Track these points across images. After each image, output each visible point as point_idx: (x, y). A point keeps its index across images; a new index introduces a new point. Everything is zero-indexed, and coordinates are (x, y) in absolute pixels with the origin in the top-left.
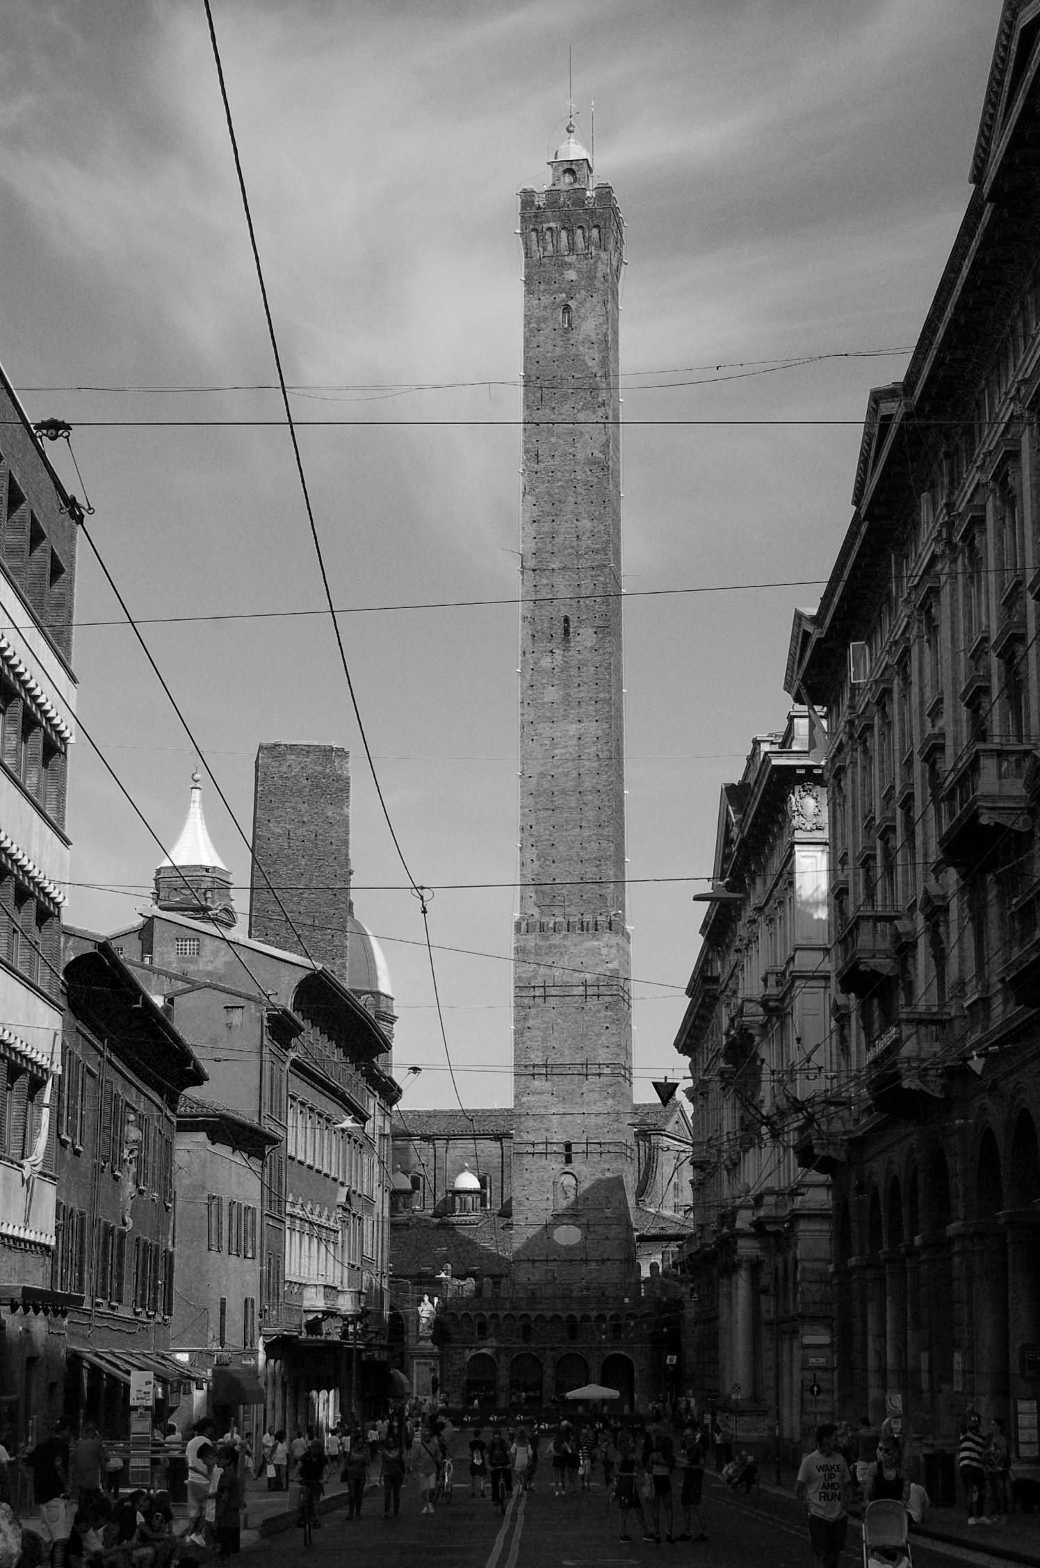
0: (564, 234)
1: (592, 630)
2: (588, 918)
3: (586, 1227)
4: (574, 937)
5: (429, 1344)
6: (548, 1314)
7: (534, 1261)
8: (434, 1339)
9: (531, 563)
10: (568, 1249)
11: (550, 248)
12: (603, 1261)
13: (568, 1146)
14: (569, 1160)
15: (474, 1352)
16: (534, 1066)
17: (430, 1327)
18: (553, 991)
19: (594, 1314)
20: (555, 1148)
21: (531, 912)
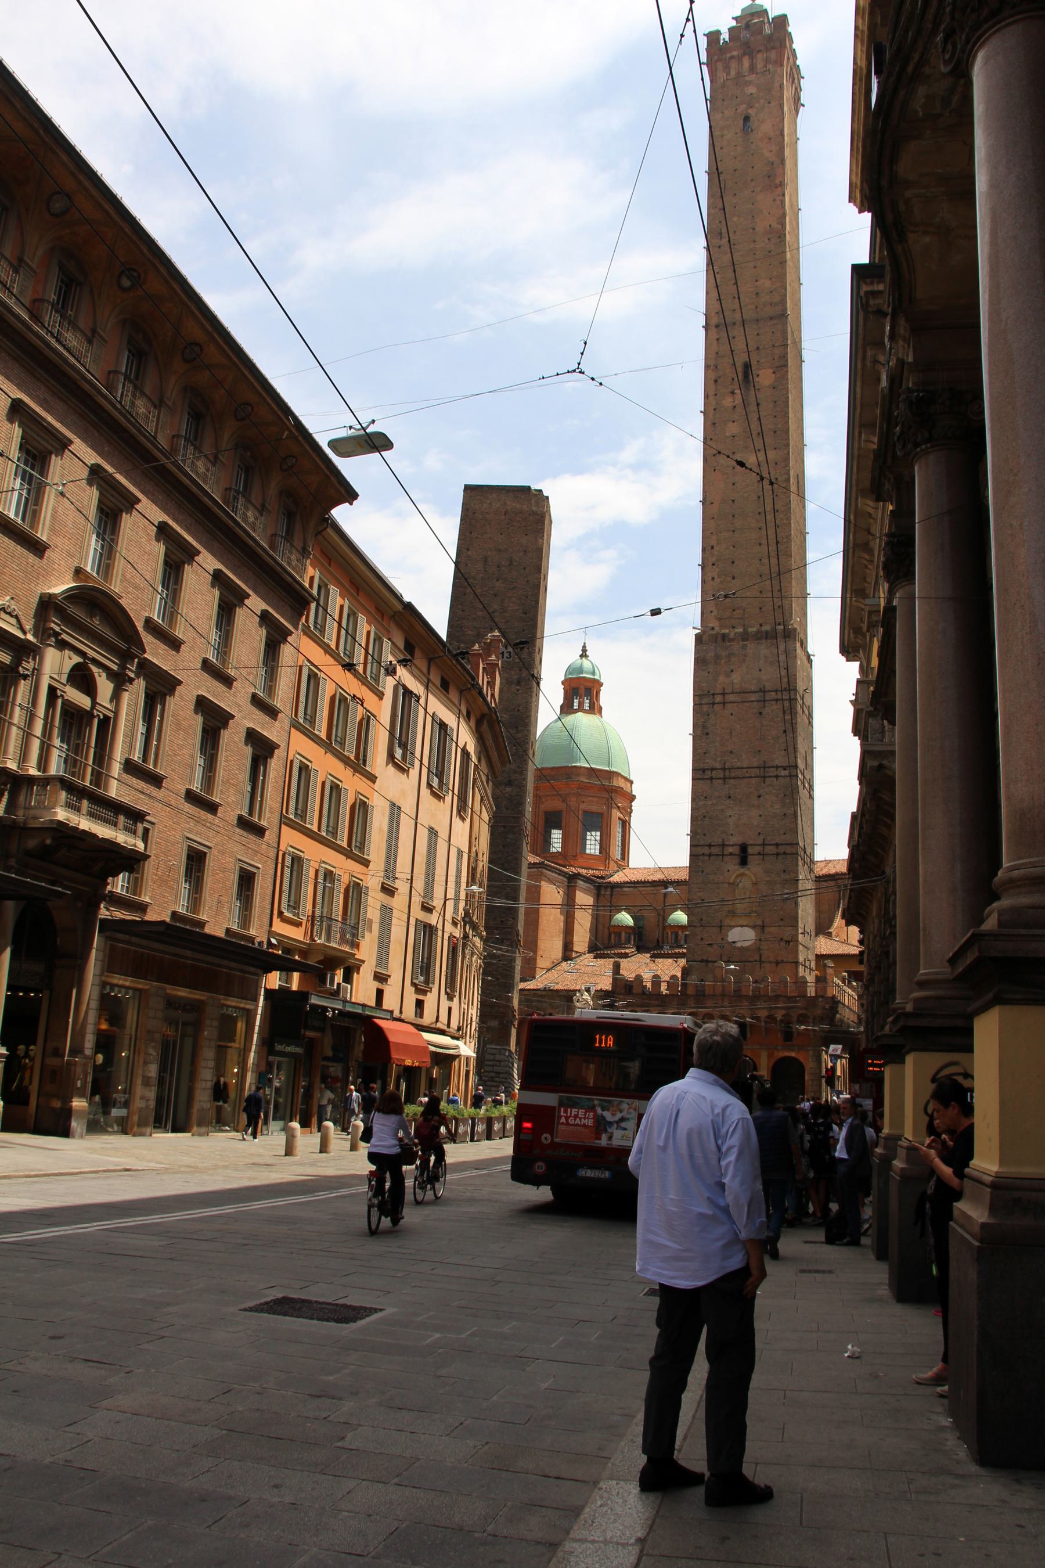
0: (746, 63)
1: (771, 371)
2: (767, 628)
4: (751, 646)
7: (707, 961)
9: (714, 321)
11: (733, 73)
13: (744, 848)
14: (744, 862)
16: (712, 769)
18: (731, 698)
20: (730, 850)
21: (711, 625)
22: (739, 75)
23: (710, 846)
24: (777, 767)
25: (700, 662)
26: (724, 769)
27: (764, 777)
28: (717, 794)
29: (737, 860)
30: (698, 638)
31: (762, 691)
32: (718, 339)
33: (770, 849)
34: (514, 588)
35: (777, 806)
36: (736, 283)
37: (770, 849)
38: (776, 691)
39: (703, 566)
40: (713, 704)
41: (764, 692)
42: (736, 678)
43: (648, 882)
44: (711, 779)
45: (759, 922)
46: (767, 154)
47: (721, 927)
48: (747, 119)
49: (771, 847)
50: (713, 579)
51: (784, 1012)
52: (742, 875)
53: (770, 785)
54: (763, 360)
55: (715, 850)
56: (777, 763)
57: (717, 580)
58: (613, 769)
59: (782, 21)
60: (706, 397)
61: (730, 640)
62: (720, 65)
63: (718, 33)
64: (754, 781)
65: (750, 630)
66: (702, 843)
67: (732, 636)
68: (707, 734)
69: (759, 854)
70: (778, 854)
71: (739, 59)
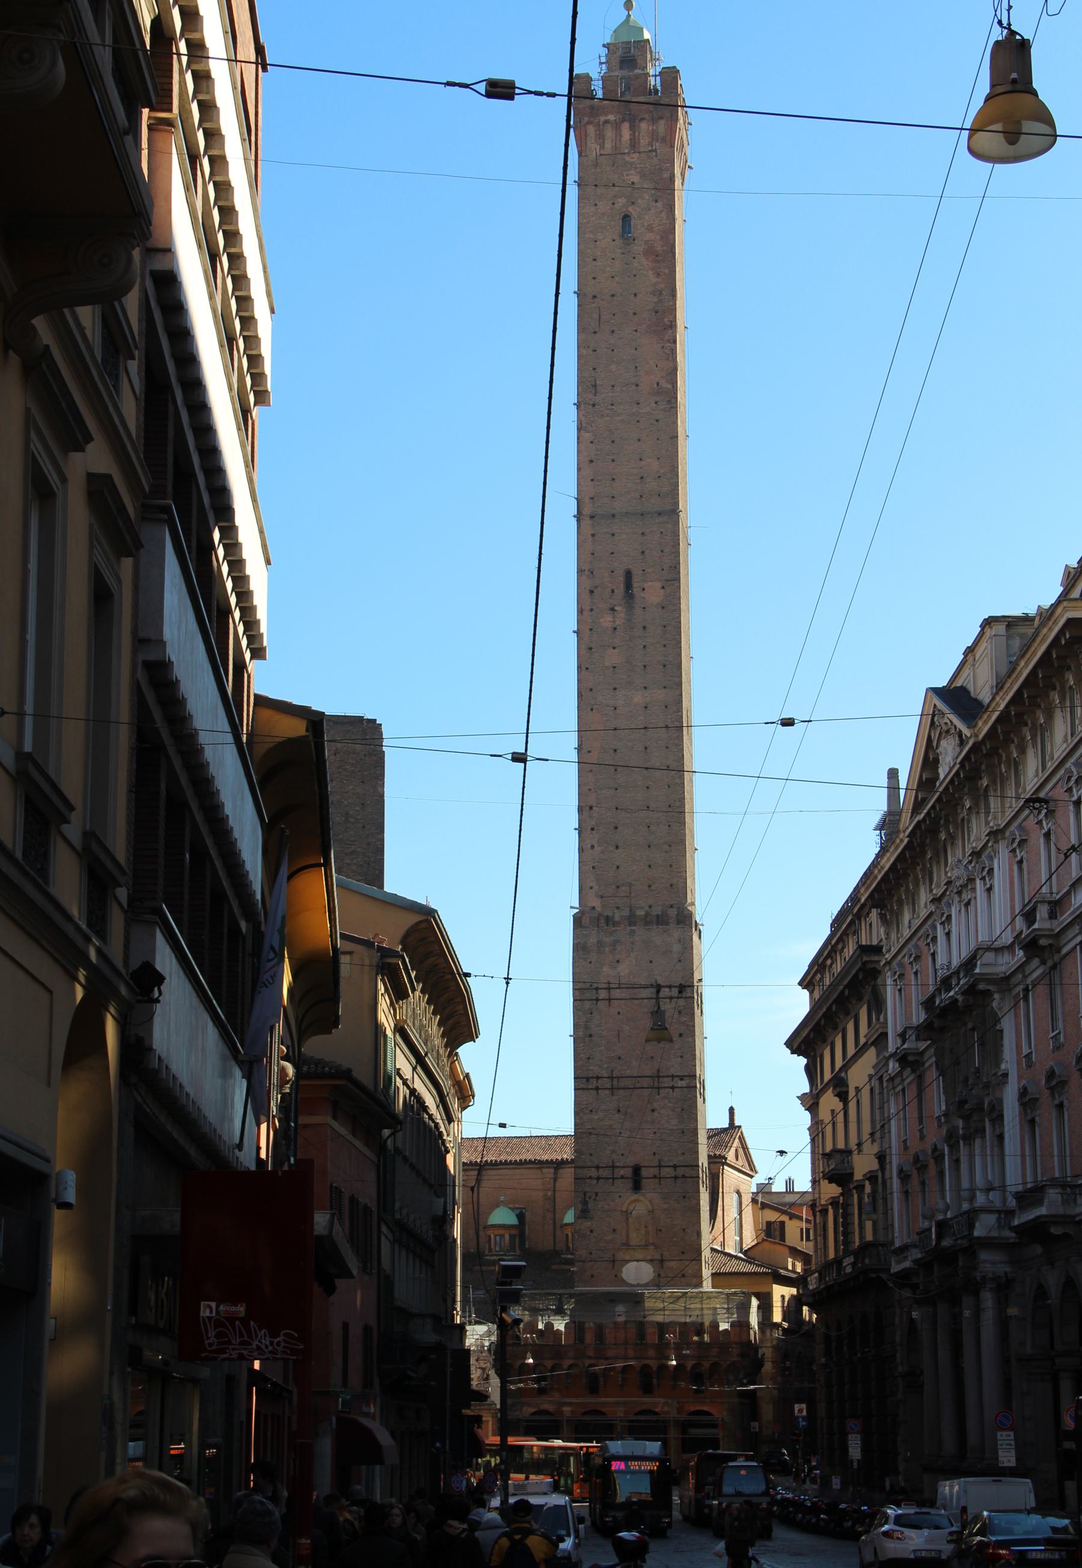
0: (625, 129)
1: (658, 585)
2: (657, 911)
9: (587, 511)
11: (608, 145)
13: (637, 1170)
14: (637, 1186)
16: (598, 1078)
18: (616, 993)
20: (622, 1172)
22: (617, 151)
23: (598, 1167)
24: (673, 1076)
25: (580, 949)
27: (659, 1088)
28: (603, 1107)
29: (629, 1184)
30: (578, 921)
32: (593, 535)
34: (353, 853)
35: (674, 1122)
37: (666, 1172)
39: (580, 830)
40: (597, 1000)
42: (623, 969)
44: (597, 1089)
45: (657, 1256)
47: (614, 1261)
48: (626, 218)
49: (668, 1170)
50: (593, 847)
52: (636, 1201)
53: (664, 1098)
54: (650, 570)
55: (604, 1173)
56: (672, 1071)
57: (598, 849)
60: (580, 611)
61: (615, 924)
62: (591, 129)
64: (646, 1092)
66: (589, 1164)
67: (617, 918)
68: (591, 1036)
69: (655, 1177)
70: (676, 1178)
71: (617, 126)
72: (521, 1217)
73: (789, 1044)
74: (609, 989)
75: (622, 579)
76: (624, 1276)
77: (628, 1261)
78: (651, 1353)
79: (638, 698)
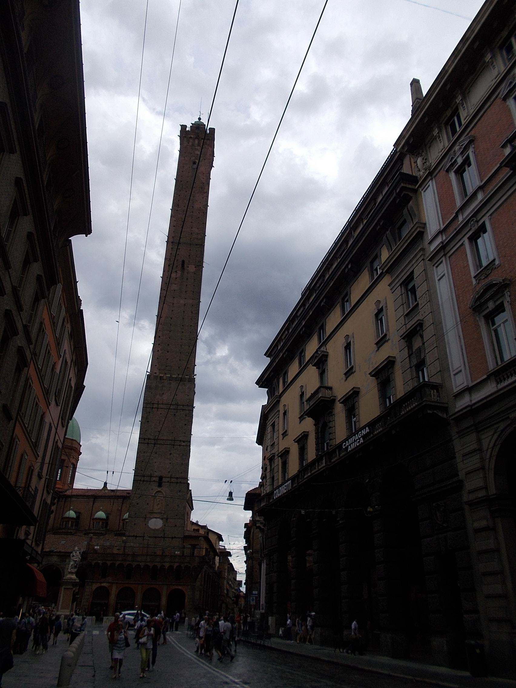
0: (196, 141)
3: (166, 520)
5: (74, 576)
6: (142, 564)
7: (136, 537)
8: (77, 574)
9: (171, 240)
10: (155, 530)
11: (190, 144)
12: (172, 538)
13: (161, 478)
14: (160, 485)
15: (98, 585)
16: (149, 439)
17: (76, 567)
19: (167, 565)
20: (154, 479)
22: (193, 145)
24: (180, 441)
26: (154, 439)
31: (177, 405)
33: (173, 480)
36: (182, 227)
37: (173, 480)
38: (183, 406)
40: (153, 408)
41: (178, 405)
43: (85, 496)
44: (148, 443)
45: (165, 516)
46: (202, 179)
47: (145, 518)
51: (177, 564)
55: (146, 479)
56: (180, 439)
58: (74, 439)
59: (213, 130)
60: (164, 271)
61: (163, 380)
63: (186, 126)
65: (173, 376)
67: (165, 378)
70: (177, 483)
72: (107, 517)
73: (257, 383)
74: (158, 404)
75: (181, 263)
76: (149, 525)
77: (152, 518)
78: (158, 559)
79: (182, 302)
